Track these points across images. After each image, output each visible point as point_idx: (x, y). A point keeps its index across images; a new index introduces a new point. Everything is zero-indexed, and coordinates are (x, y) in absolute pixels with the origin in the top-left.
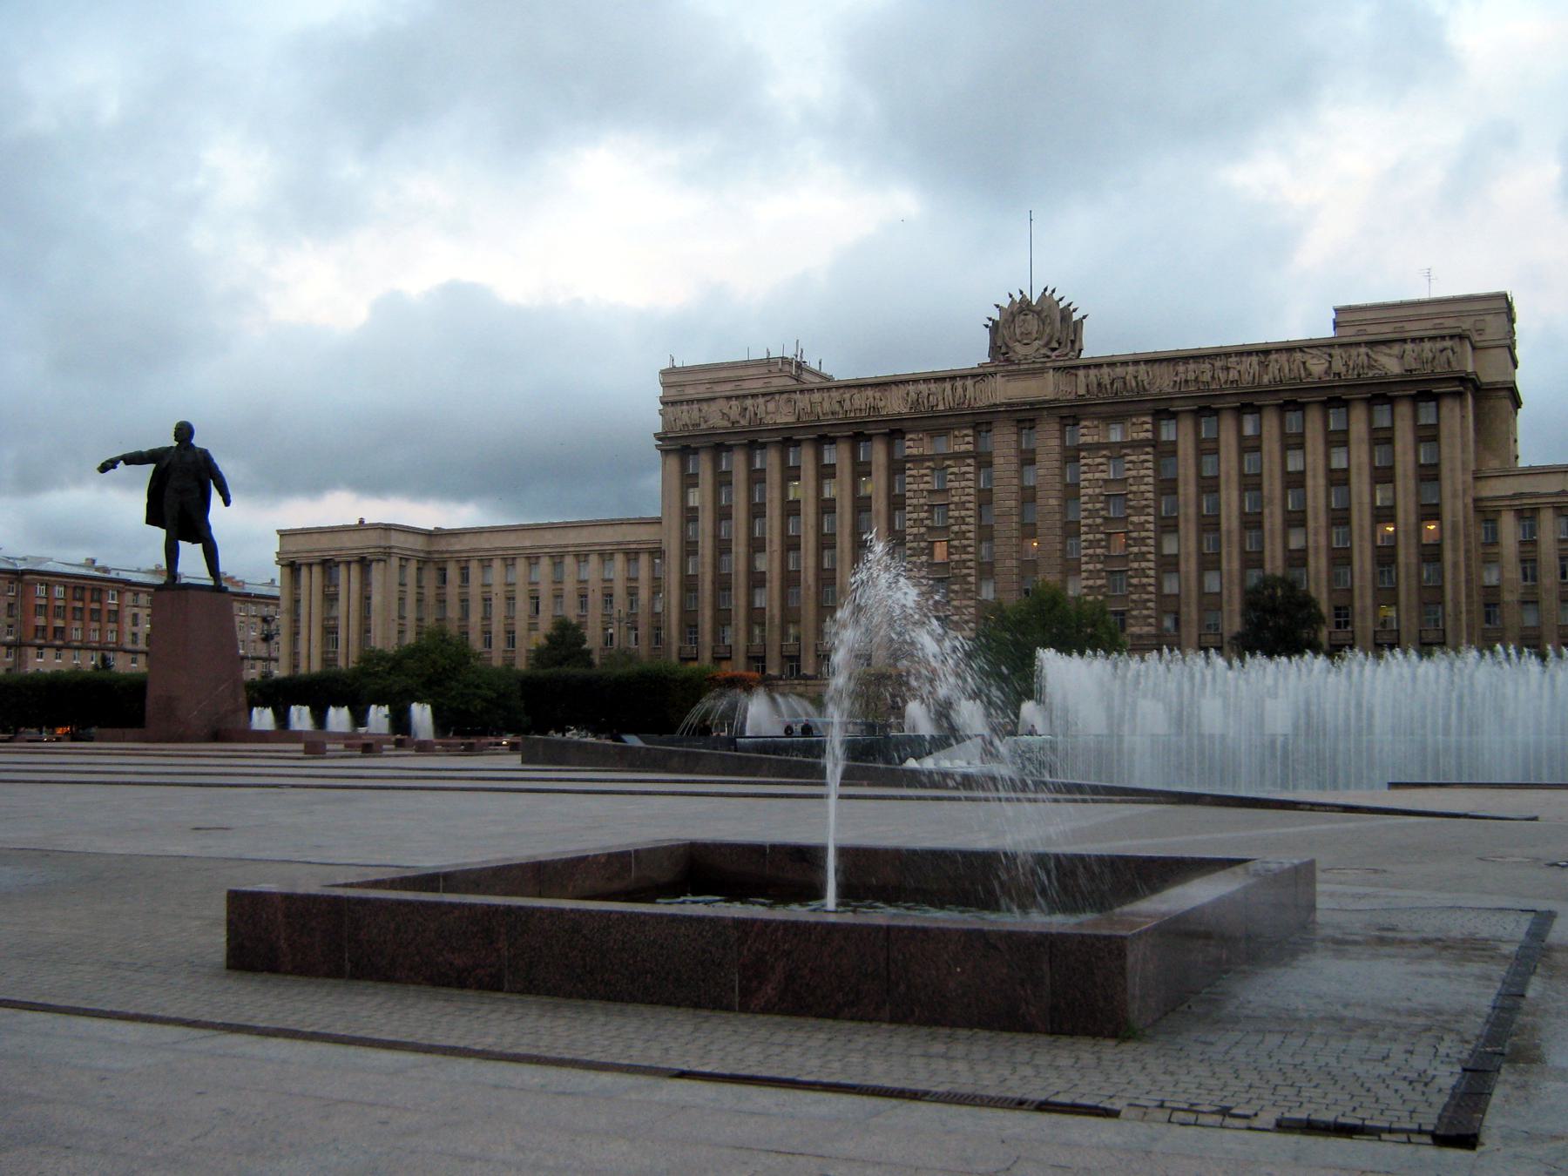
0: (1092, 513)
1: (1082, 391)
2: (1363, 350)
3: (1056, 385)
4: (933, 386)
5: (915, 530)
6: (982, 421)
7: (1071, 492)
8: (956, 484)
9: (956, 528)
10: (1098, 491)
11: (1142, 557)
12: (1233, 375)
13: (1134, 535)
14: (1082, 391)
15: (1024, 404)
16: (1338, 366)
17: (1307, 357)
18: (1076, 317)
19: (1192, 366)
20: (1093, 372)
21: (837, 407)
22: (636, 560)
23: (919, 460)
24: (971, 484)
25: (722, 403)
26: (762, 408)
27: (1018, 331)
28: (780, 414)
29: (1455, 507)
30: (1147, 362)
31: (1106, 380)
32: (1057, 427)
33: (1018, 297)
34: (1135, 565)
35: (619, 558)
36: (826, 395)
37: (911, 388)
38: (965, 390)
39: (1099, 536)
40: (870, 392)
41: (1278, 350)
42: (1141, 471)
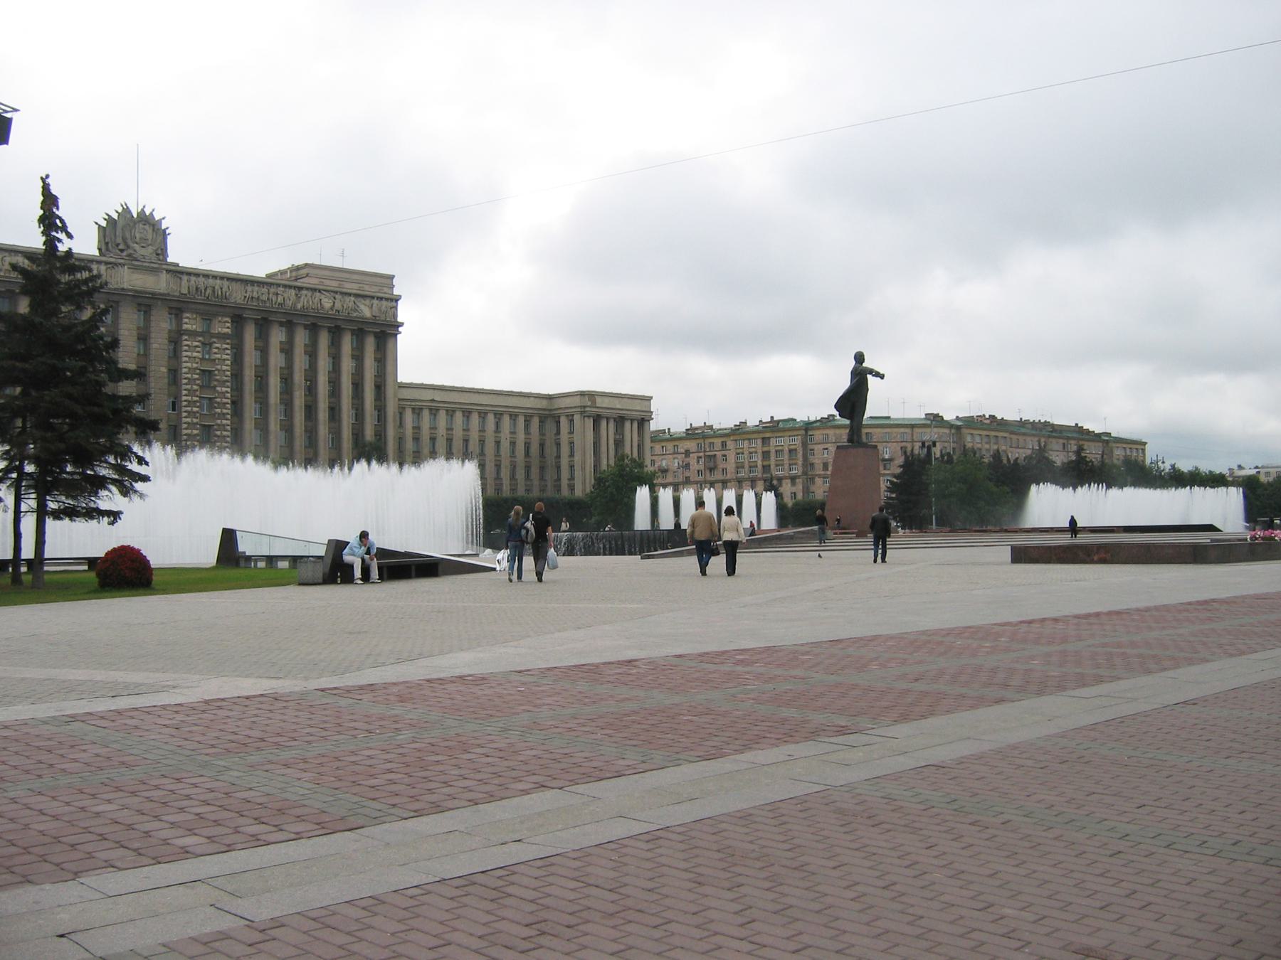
0: (191, 381)
1: (185, 291)
3: (168, 284)
12: (280, 299)
16: (338, 305)
19: (256, 288)
20: (193, 278)
27: (138, 235)
30: (228, 279)
32: (166, 314)
41: (307, 289)
42: (223, 355)
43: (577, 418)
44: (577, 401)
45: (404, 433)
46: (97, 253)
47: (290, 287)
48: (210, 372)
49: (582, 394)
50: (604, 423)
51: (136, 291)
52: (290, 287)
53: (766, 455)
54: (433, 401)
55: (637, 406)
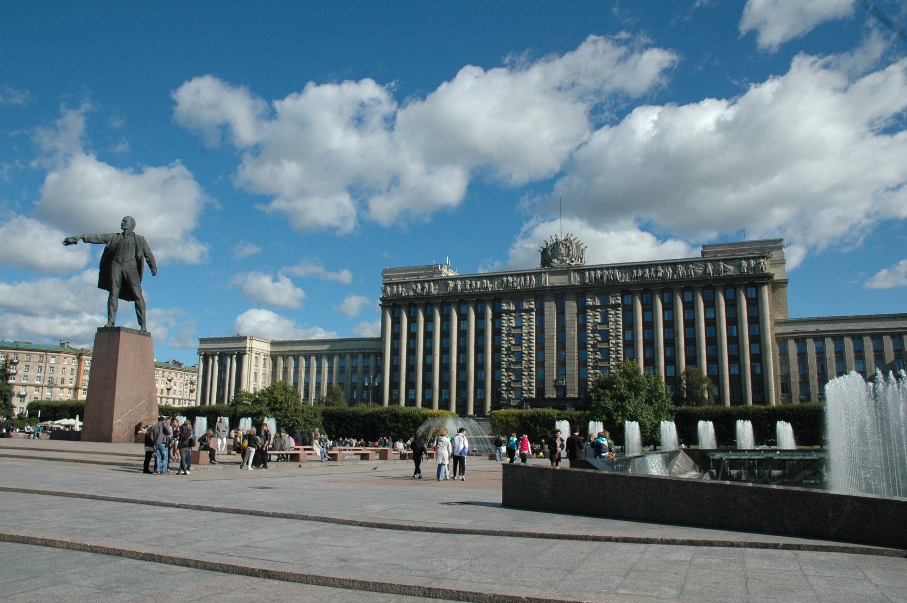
7: (582, 328)
14: (587, 281)
18: (582, 247)
22: (369, 357)
23: (508, 312)
33: (554, 238)
35: (360, 356)
38: (531, 279)
42: (616, 318)
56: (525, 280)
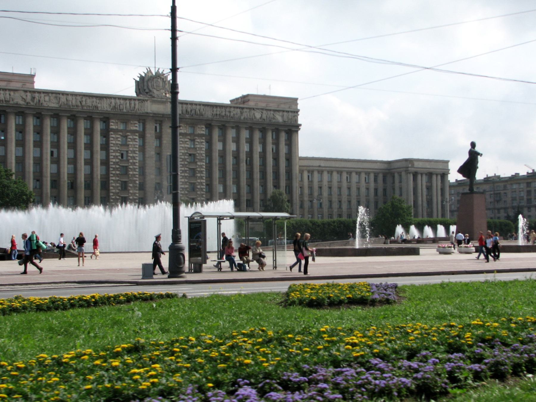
0: (184, 160)
2: (272, 112)
4: (122, 101)
5: (114, 160)
6: (143, 118)
8: (131, 143)
9: (131, 161)
10: (186, 151)
11: (201, 178)
13: (199, 169)
15: (160, 114)
16: (264, 116)
17: (255, 112)
19: (218, 109)
20: (185, 106)
21: (79, 104)
23: (116, 131)
24: (137, 143)
25: (23, 94)
26: (42, 98)
27: (155, 85)
28: (53, 104)
29: (296, 170)
31: (189, 110)
34: (199, 181)
36: (74, 97)
37: (113, 101)
38: (135, 105)
39: (186, 169)
40: (94, 100)
43: (403, 174)
44: (404, 164)
45: (303, 185)
46: (134, 95)
47: (237, 108)
48: (194, 155)
49: (406, 160)
50: (419, 177)
51: (155, 114)
52: (237, 108)
53: (529, 192)
54: (320, 166)
55: (441, 166)
56: (130, 104)
